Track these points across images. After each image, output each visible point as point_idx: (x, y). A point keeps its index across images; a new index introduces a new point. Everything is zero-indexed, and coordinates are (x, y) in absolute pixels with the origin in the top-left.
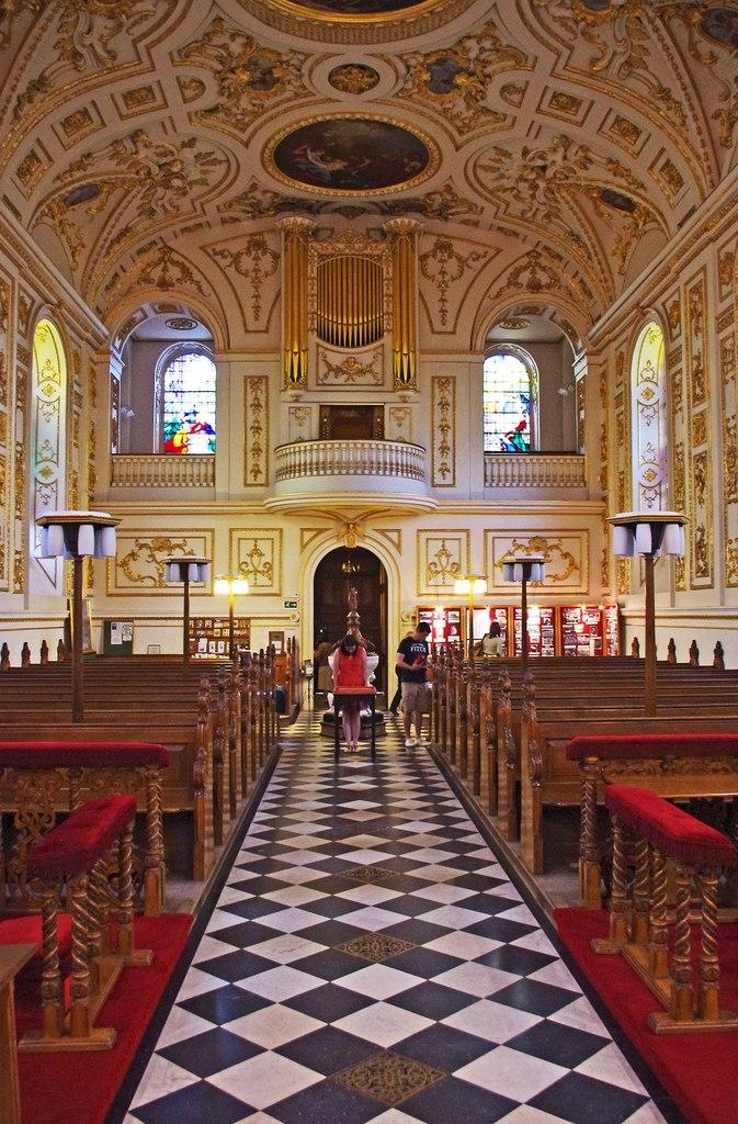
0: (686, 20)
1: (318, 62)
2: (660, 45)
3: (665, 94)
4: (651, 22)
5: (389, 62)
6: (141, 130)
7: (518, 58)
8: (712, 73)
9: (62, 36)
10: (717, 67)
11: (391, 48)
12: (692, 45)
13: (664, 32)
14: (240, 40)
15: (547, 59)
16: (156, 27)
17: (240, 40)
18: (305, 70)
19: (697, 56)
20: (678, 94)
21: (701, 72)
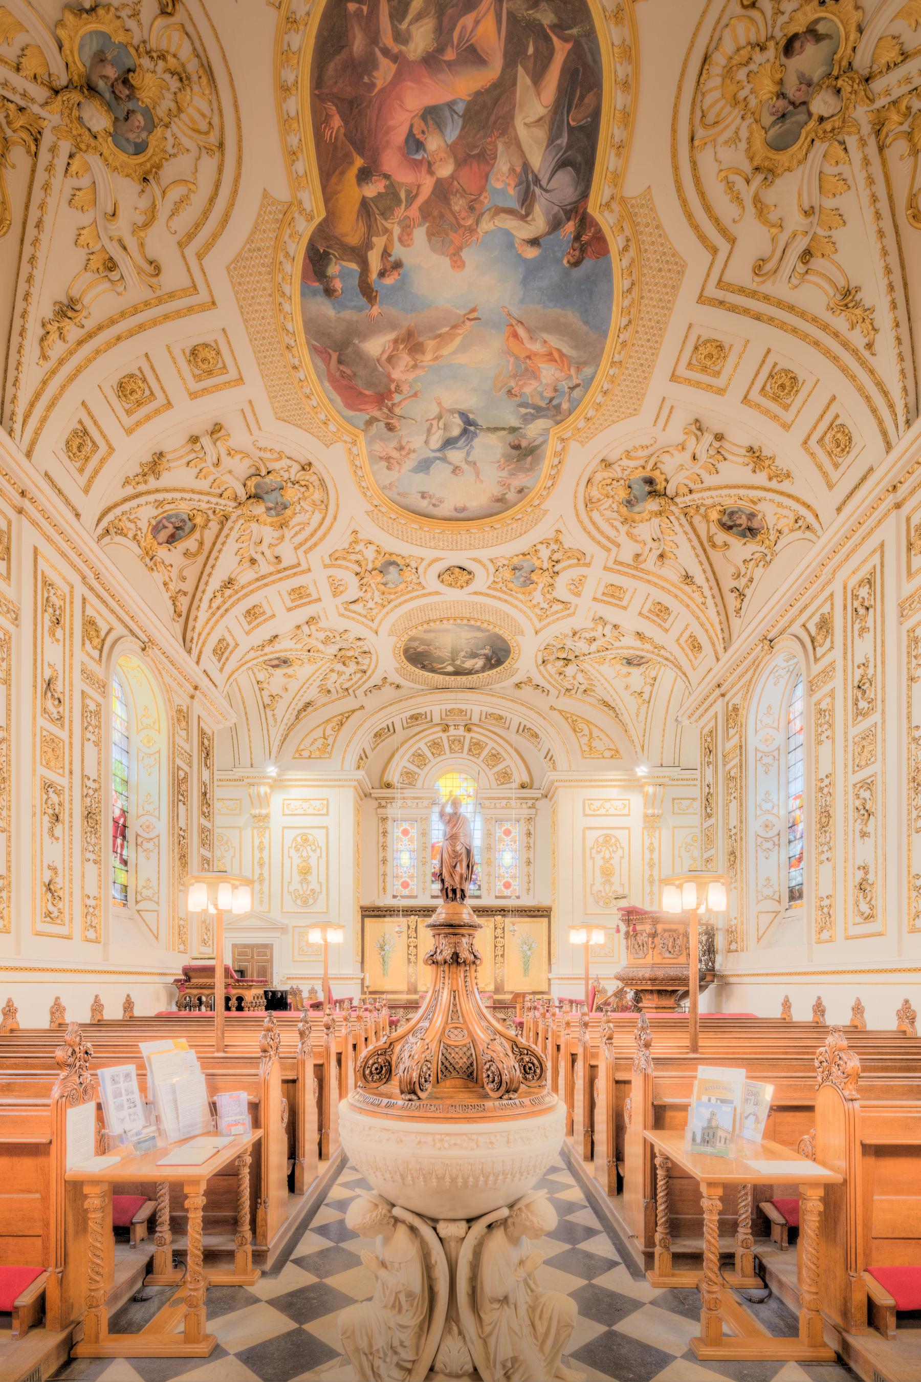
0: (706, 517)
1: (429, 565)
2: (685, 538)
3: (688, 578)
4: (678, 519)
5: (484, 565)
6: (157, 275)
7: (580, 558)
8: (724, 555)
9: (240, 545)
10: (727, 553)
11: (485, 554)
12: (710, 539)
13: (688, 528)
14: (372, 548)
15: (599, 557)
16: (312, 535)
17: (372, 548)
18: (420, 570)
19: (714, 546)
20: (700, 579)
21: (715, 555)
